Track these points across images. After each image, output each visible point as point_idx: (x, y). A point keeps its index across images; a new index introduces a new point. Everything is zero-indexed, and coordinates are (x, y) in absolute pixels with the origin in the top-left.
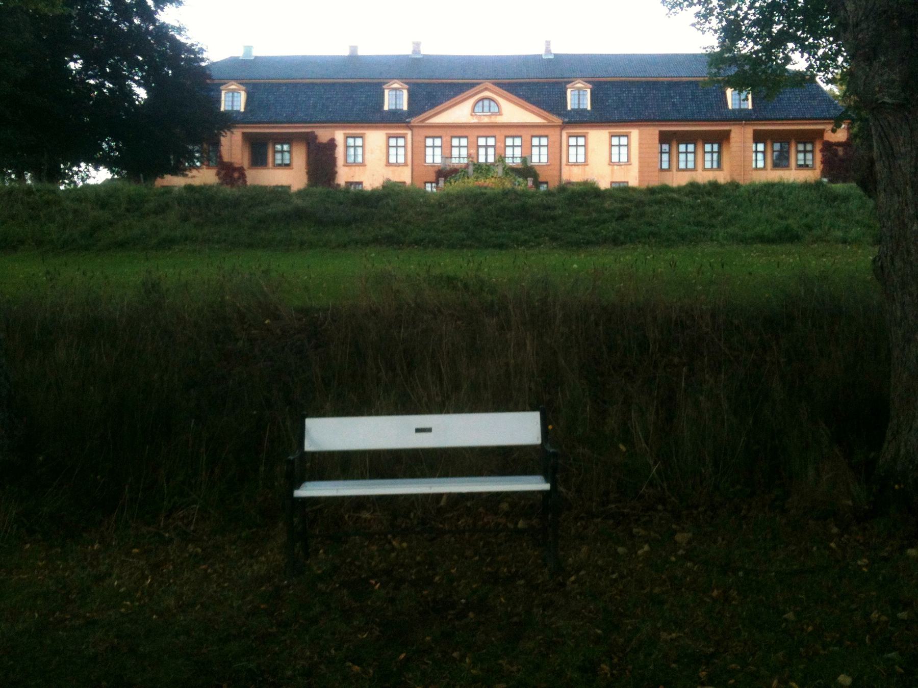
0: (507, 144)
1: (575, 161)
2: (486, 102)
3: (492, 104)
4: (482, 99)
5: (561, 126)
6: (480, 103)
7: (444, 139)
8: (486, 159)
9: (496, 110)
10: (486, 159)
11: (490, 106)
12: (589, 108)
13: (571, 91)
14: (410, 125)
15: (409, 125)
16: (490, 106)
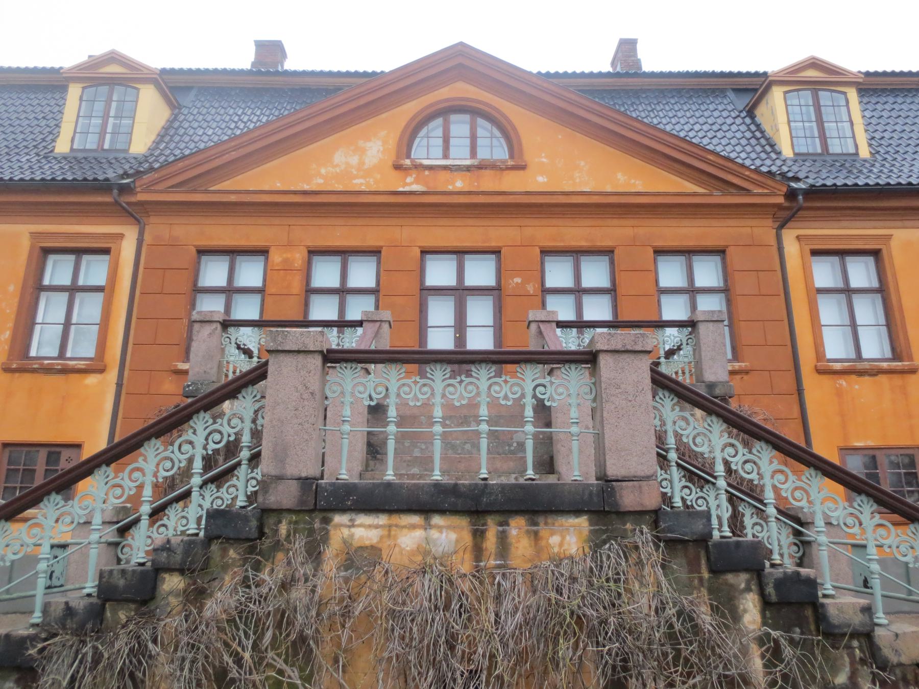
0: (550, 283)
1: (853, 355)
2: (460, 127)
3: (484, 129)
4: (446, 111)
5: (779, 207)
6: (435, 127)
7: (276, 257)
8: (461, 338)
9: (500, 153)
10: (461, 338)
11: (473, 138)
12: (865, 152)
13: (786, 93)
14: (133, 199)
15: (125, 199)
16: (473, 138)
